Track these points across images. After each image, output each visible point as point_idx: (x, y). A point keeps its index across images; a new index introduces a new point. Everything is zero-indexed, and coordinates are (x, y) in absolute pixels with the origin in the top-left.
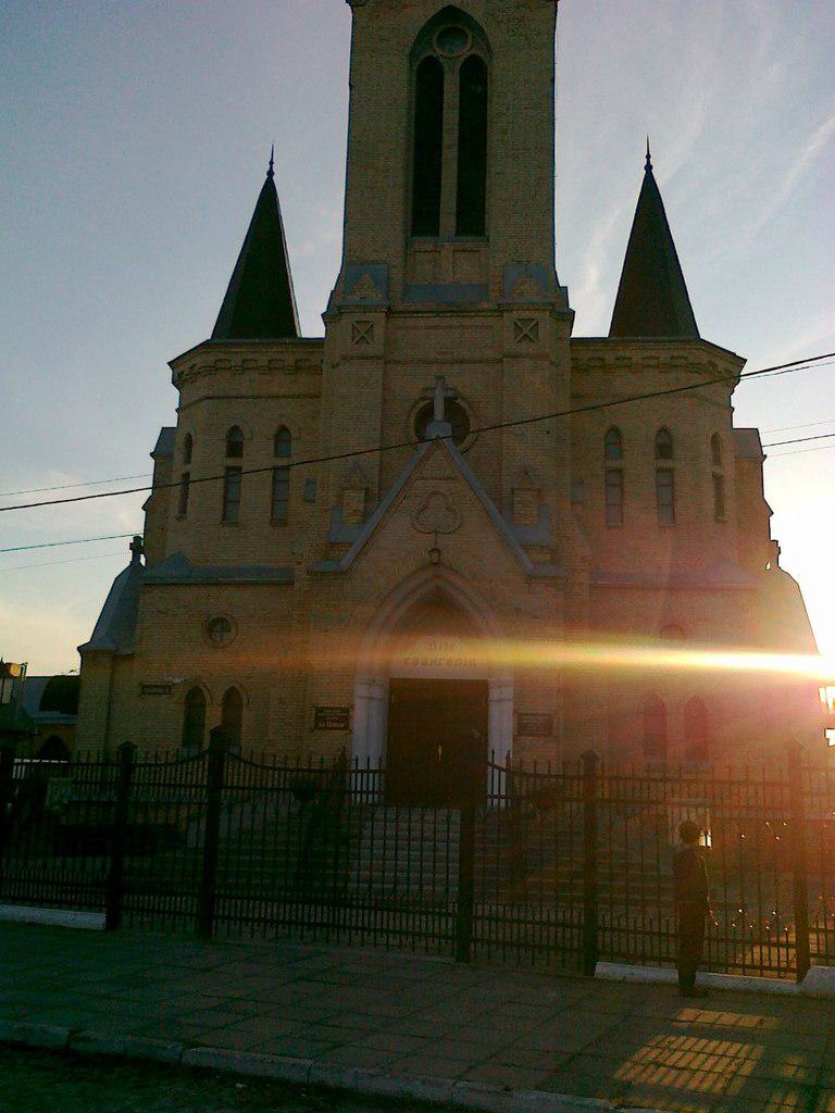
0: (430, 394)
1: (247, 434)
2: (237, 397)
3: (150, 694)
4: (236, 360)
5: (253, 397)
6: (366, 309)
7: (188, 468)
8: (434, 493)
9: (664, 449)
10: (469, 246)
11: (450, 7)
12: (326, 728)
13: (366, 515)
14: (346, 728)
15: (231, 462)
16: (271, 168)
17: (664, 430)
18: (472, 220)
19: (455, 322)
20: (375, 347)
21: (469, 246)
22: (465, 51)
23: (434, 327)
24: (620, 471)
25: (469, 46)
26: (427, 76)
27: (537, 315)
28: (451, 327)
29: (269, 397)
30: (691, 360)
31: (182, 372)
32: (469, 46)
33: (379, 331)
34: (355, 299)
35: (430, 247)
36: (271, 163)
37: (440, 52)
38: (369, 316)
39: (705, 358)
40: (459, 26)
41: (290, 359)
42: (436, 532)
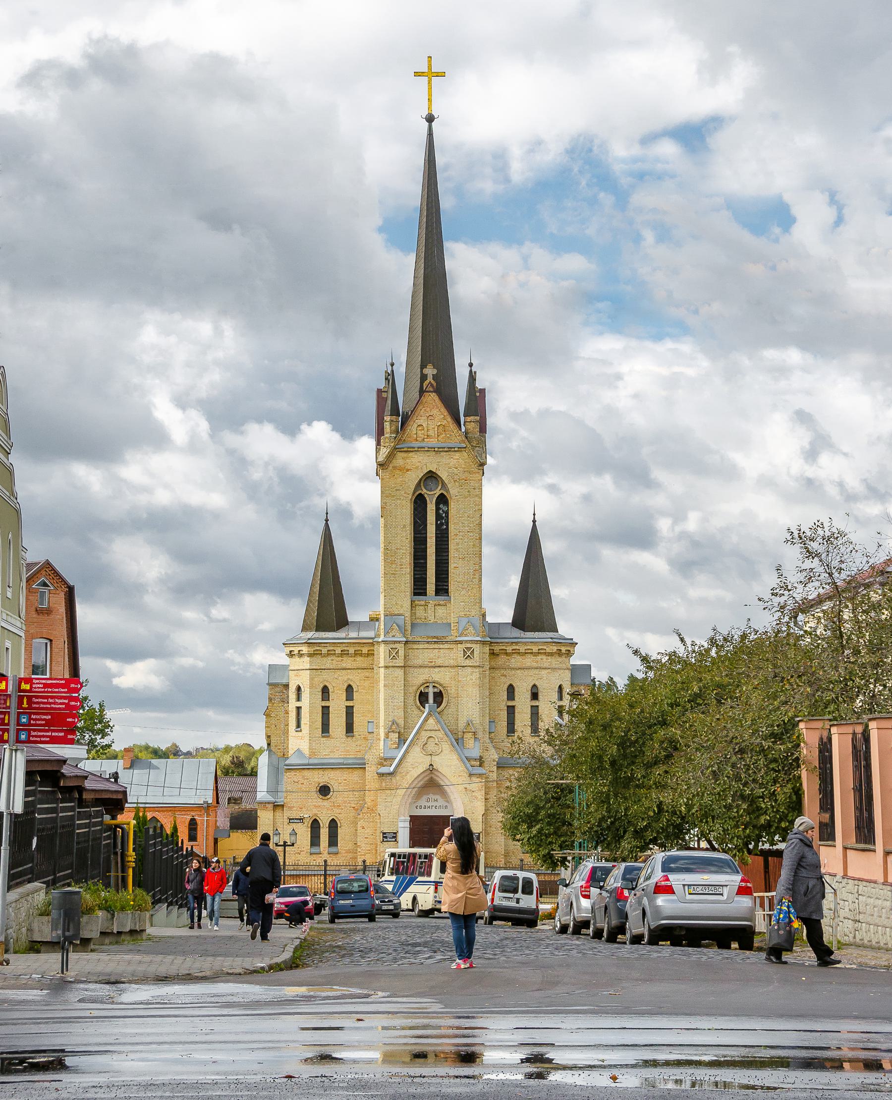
0: (426, 691)
4: (324, 651)
7: (298, 704)
8: (431, 737)
9: (535, 696)
10: (442, 603)
11: (430, 471)
12: (387, 841)
13: (399, 747)
14: (396, 841)
15: (325, 704)
16: (327, 516)
17: (534, 686)
18: (442, 589)
19: (436, 646)
21: (442, 603)
22: (438, 492)
23: (427, 649)
24: (513, 707)
25: (440, 487)
26: (419, 503)
27: (473, 646)
28: (435, 649)
30: (548, 650)
32: (440, 487)
33: (401, 653)
35: (423, 603)
37: (425, 491)
38: (397, 646)
39: (555, 649)
41: (352, 651)
42: (431, 755)
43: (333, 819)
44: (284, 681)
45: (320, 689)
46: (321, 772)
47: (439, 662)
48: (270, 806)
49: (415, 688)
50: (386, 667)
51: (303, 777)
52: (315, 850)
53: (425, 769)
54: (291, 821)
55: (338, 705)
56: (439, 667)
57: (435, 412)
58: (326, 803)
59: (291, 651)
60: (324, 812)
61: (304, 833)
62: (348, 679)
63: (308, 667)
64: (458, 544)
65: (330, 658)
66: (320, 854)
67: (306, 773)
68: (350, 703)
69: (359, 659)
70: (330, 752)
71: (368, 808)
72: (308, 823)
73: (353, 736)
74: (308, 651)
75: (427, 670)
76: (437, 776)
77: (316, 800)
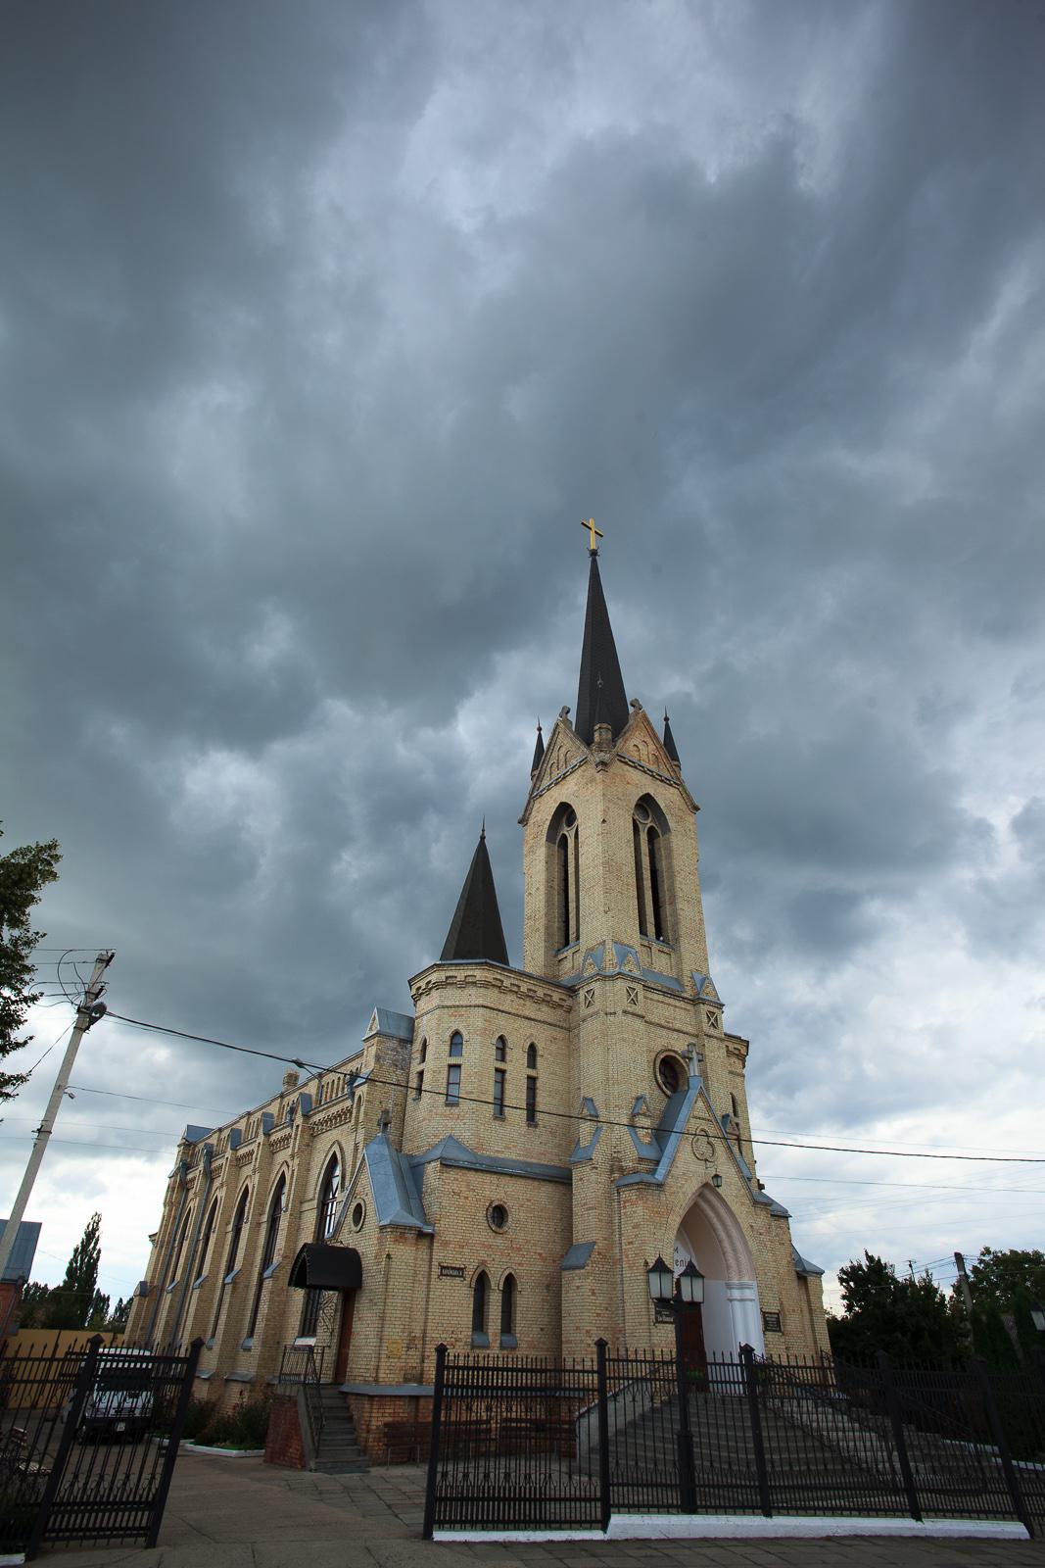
1: (509, 1044)
2: (503, 1012)
3: (447, 1275)
5: (514, 1014)
6: (634, 979)
7: (454, 1061)
11: (648, 796)
15: (500, 1065)
19: (671, 1001)
20: (638, 1009)
22: (649, 823)
23: (662, 1002)
25: (650, 819)
29: (524, 1017)
31: (456, 977)
32: (650, 819)
34: (626, 969)
36: (483, 830)
40: (645, 806)
41: (540, 993)
43: (510, 1274)
44: (403, 1034)
45: (494, 1041)
46: (494, 1178)
47: (677, 1026)
48: (411, 1236)
49: (654, 1055)
50: (625, 1012)
51: (468, 1186)
52: (479, 1339)
53: (700, 1185)
54: (445, 1272)
55: (517, 1067)
56: (675, 1030)
57: (648, 740)
58: (499, 1241)
59: (447, 978)
60: (497, 1259)
61: (457, 1298)
62: (532, 1035)
63: (480, 1002)
64: (681, 883)
65: (510, 997)
66: (488, 1348)
67: (471, 1175)
68: (532, 1073)
69: (545, 1008)
70: (505, 1147)
71: (599, 1254)
72: (471, 1273)
73: (536, 1126)
74: (486, 977)
75: (664, 1032)
76: (709, 1202)
77: (481, 1233)
